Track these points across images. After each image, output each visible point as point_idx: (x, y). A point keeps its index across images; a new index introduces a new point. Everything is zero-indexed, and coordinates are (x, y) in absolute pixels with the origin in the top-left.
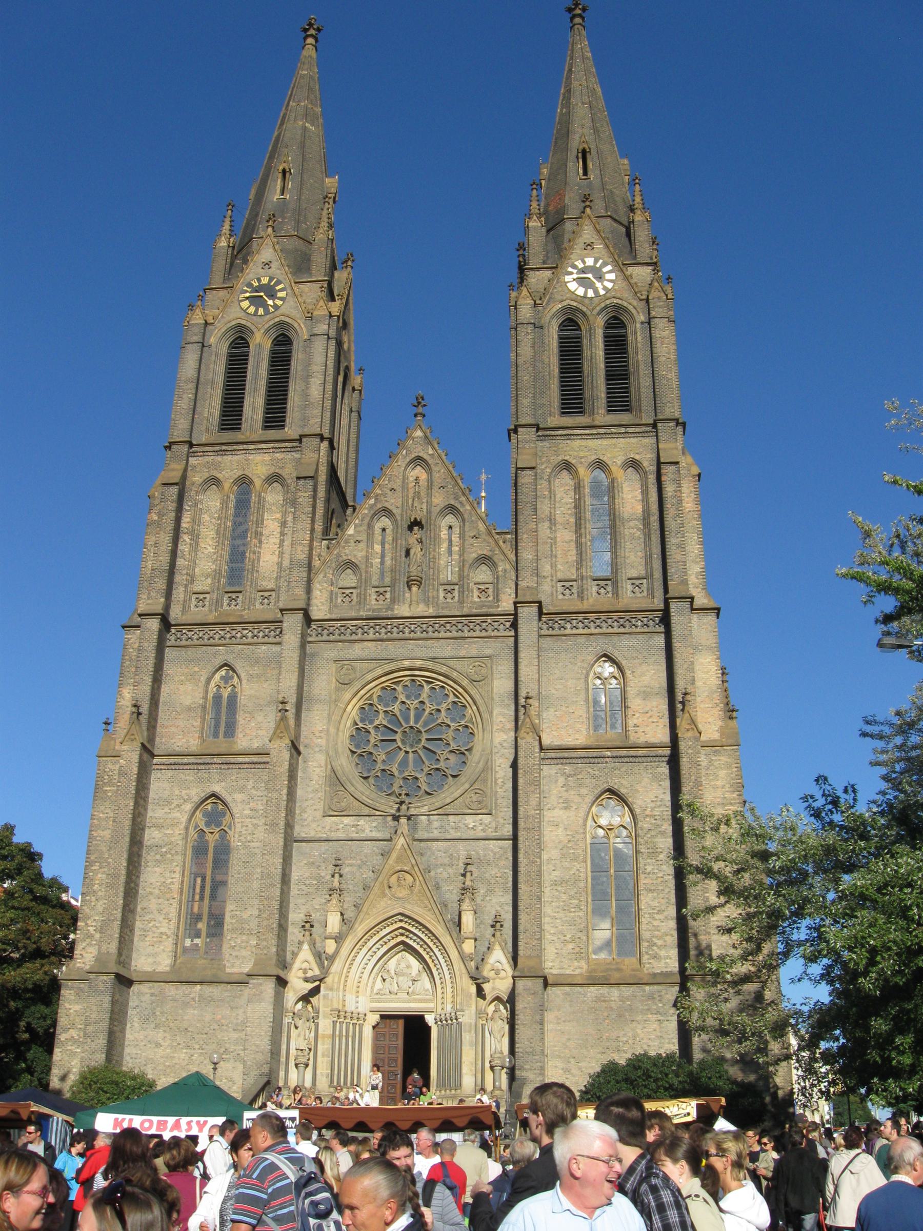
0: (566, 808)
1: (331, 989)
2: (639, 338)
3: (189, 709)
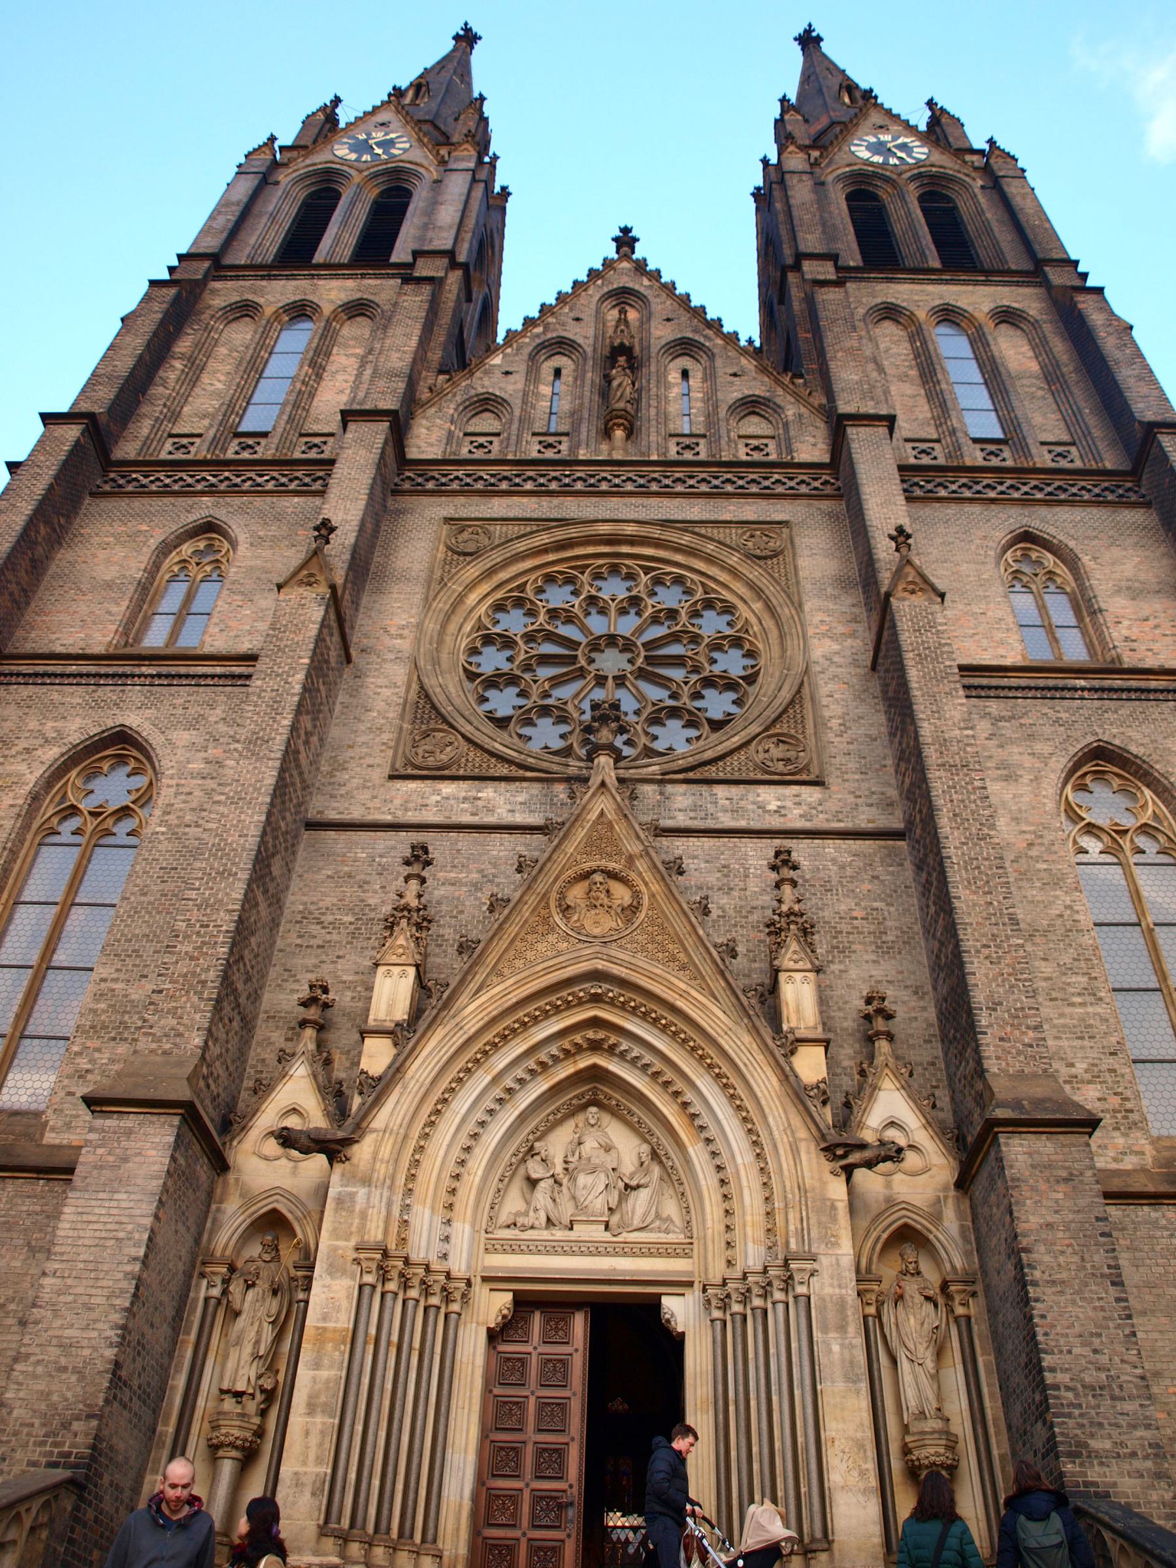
0: (1007, 778)
1: (367, 1181)
3: (109, 585)
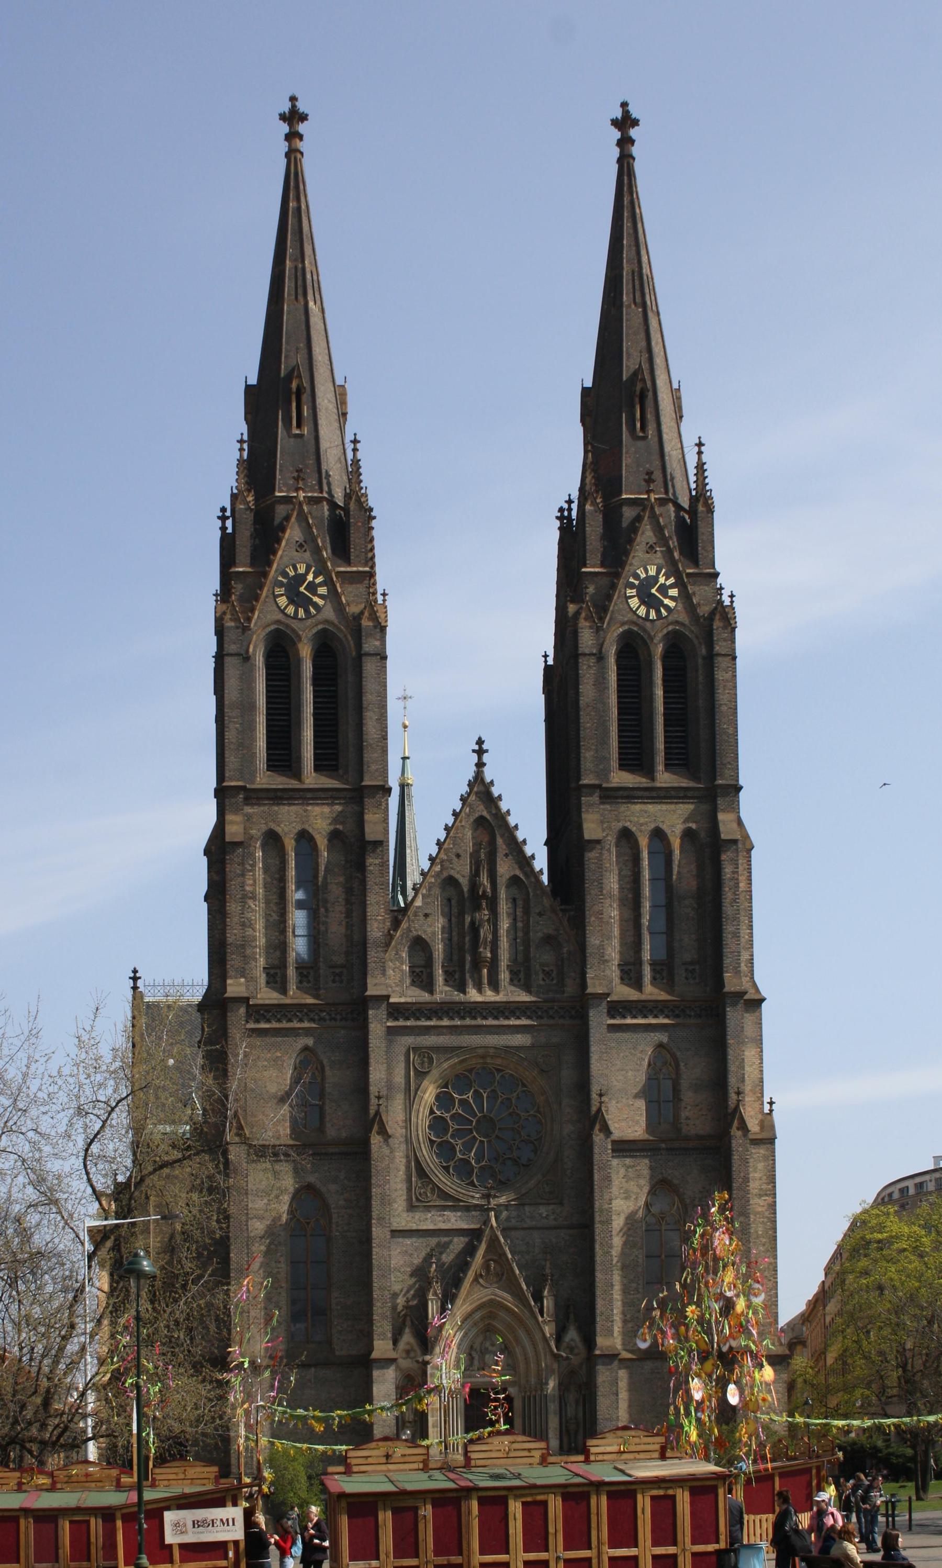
0: (626, 1198)
2: (701, 678)
